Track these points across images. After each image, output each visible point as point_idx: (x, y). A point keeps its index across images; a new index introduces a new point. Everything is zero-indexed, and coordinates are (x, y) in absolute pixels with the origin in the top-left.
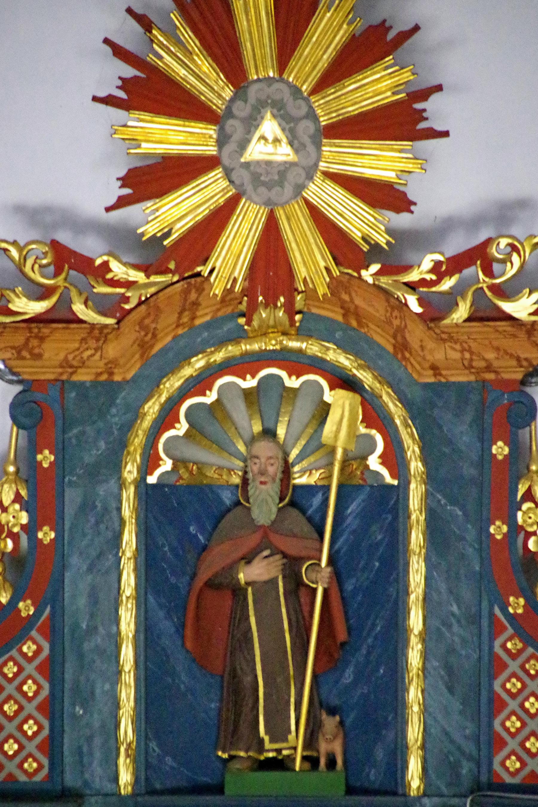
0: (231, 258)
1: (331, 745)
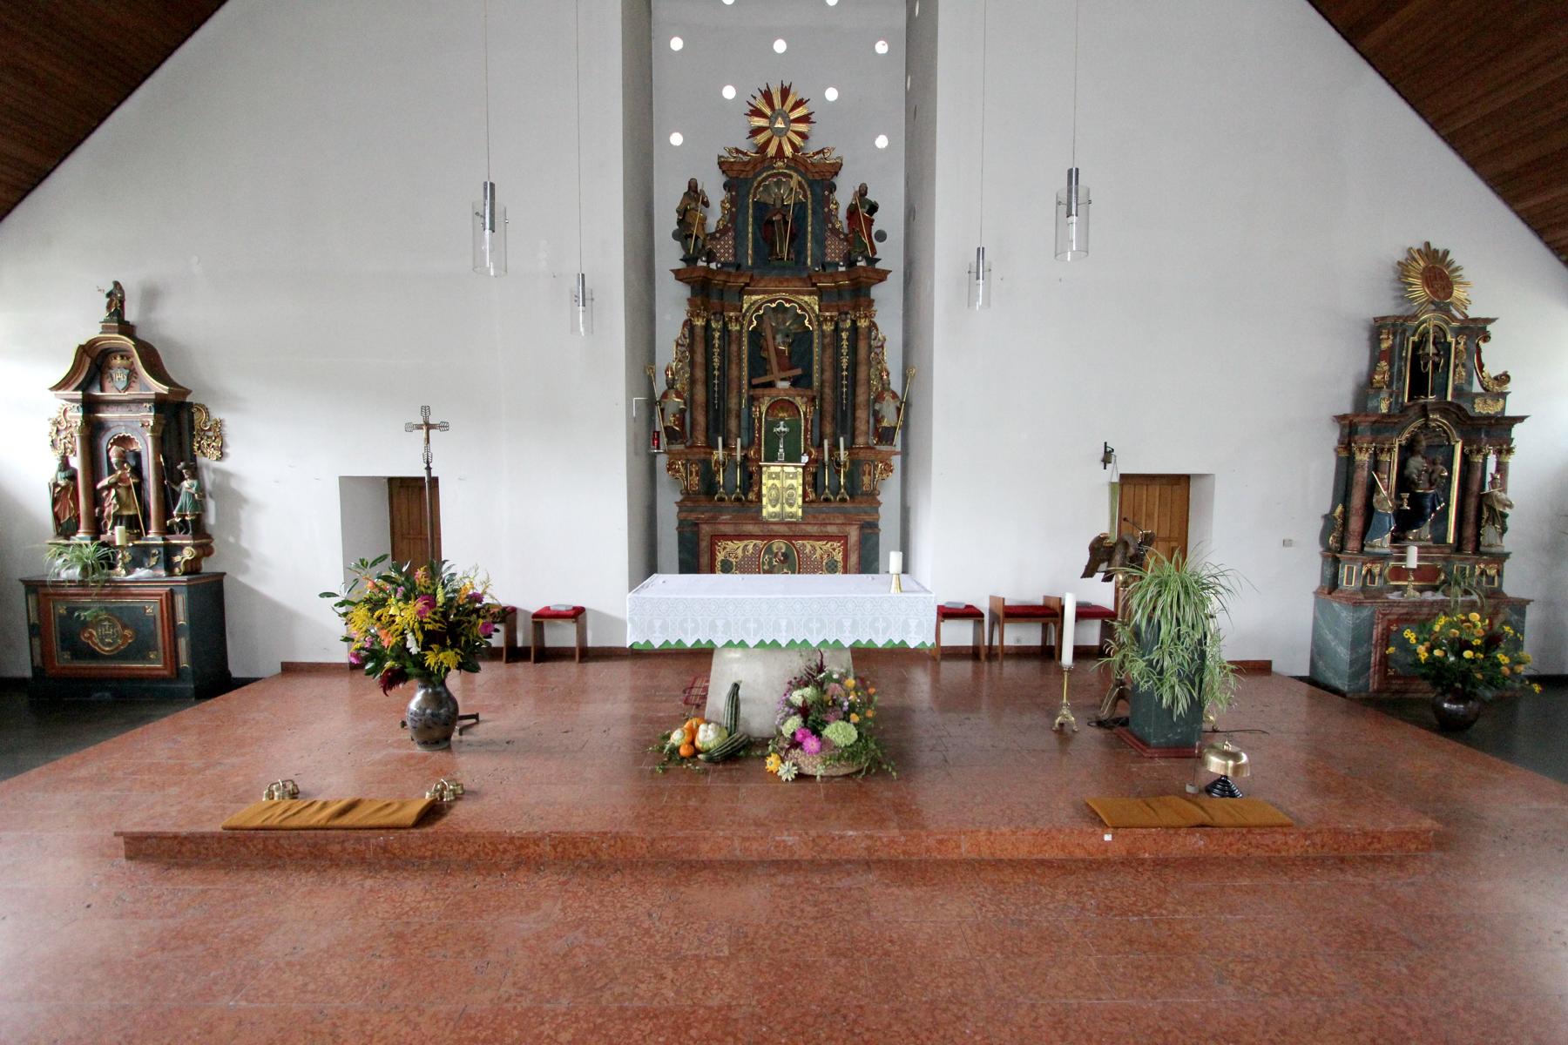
0: (772, 150)
1: (792, 256)
